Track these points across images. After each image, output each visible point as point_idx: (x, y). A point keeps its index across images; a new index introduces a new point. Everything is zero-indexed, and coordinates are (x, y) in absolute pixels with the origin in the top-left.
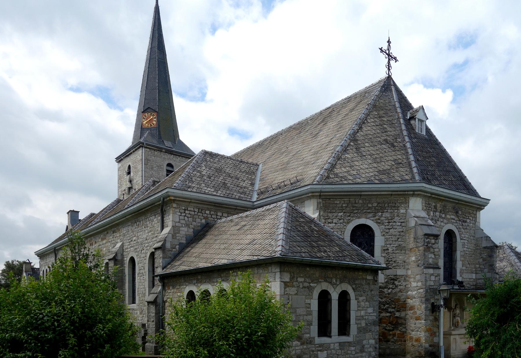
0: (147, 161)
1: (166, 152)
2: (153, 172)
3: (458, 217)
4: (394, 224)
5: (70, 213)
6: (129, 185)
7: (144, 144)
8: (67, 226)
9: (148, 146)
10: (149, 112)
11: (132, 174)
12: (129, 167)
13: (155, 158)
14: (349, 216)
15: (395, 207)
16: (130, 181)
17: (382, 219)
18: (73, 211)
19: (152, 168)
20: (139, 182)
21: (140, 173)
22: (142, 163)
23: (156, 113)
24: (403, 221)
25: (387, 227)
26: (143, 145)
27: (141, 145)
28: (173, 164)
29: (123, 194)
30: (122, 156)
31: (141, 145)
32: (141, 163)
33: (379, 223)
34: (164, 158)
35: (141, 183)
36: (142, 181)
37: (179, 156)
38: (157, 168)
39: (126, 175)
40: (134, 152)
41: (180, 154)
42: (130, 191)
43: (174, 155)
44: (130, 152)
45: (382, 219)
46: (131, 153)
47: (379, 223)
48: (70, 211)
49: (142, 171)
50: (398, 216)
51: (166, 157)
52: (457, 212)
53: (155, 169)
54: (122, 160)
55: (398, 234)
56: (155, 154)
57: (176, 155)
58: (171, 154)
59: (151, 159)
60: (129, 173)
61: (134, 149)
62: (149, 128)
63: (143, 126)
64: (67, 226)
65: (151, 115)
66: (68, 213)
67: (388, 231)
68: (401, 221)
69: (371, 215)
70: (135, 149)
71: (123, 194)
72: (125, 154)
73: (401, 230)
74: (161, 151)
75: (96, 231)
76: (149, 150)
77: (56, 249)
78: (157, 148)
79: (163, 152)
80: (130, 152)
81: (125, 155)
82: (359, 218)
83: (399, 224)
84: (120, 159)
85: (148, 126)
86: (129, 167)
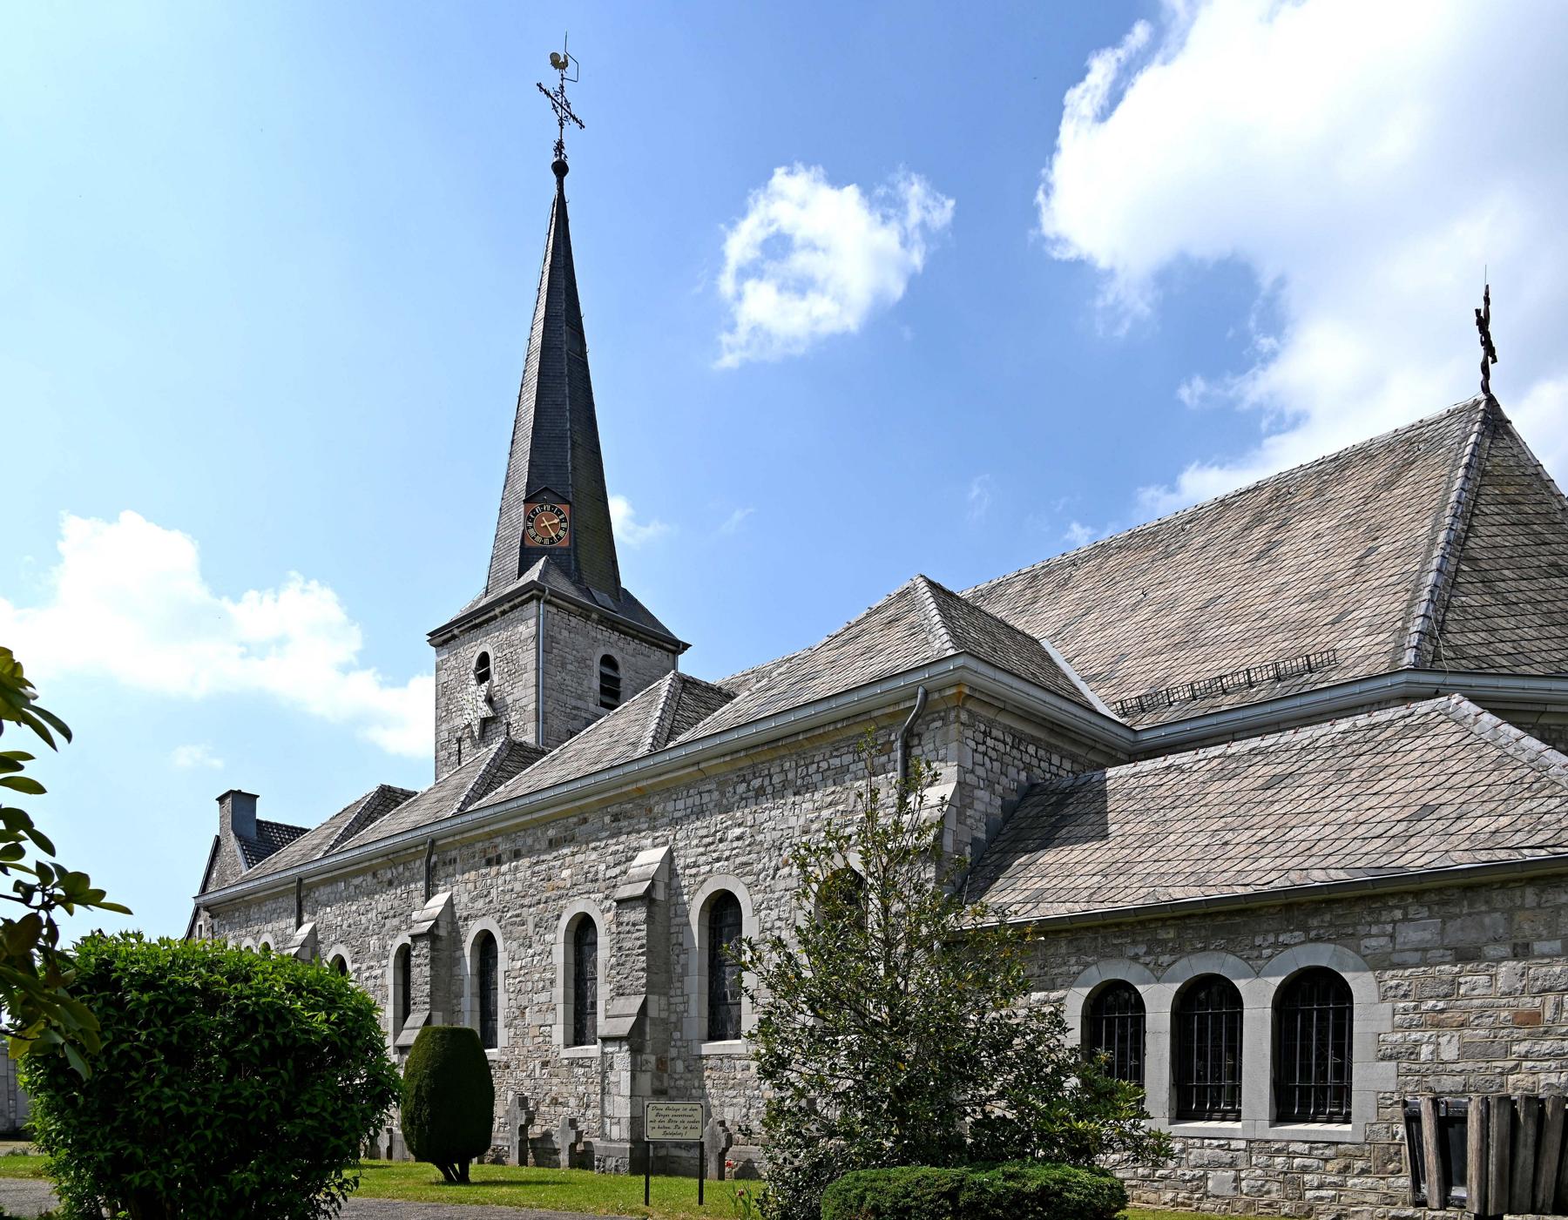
0: (546, 643)
1: (600, 622)
2: (567, 678)
5: (228, 801)
6: (486, 711)
9: (554, 599)
11: (495, 678)
12: (484, 659)
13: (572, 635)
16: (489, 700)
19: (563, 665)
20: (523, 703)
21: (530, 677)
22: (537, 648)
23: (568, 506)
26: (541, 594)
27: (534, 592)
29: (459, 740)
30: (458, 627)
31: (534, 592)
34: (595, 640)
35: (532, 706)
36: (537, 701)
38: (576, 664)
39: (474, 682)
40: (504, 613)
42: (488, 729)
43: (621, 632)
44: (492, 614)
46: (495, 617)
48: (231, 792)
49: (537, 669)
51: (599, 636)
53: (569, 667)
54: (454, 637)
56: (572, 624)
57: (626, 634)
58: (614, 629)
59: (560, 637)
61: (506, 606)
62: (545, 549)
63: (526, 542)
64: (218, 837)
65: (551, 511)
66: (221, 799)
70: (512, 603)
71: (459, 740)
72: (471, 621)
74: (588, 618)
75: (528, 817)
76: (554, 610)
77: (306, 881)
78: (579, 607)
79: (593, 621)
80: (492, 614)
81: (468, 623)
84: (449, 635)
85: (542, 543)
86: (484, 659)
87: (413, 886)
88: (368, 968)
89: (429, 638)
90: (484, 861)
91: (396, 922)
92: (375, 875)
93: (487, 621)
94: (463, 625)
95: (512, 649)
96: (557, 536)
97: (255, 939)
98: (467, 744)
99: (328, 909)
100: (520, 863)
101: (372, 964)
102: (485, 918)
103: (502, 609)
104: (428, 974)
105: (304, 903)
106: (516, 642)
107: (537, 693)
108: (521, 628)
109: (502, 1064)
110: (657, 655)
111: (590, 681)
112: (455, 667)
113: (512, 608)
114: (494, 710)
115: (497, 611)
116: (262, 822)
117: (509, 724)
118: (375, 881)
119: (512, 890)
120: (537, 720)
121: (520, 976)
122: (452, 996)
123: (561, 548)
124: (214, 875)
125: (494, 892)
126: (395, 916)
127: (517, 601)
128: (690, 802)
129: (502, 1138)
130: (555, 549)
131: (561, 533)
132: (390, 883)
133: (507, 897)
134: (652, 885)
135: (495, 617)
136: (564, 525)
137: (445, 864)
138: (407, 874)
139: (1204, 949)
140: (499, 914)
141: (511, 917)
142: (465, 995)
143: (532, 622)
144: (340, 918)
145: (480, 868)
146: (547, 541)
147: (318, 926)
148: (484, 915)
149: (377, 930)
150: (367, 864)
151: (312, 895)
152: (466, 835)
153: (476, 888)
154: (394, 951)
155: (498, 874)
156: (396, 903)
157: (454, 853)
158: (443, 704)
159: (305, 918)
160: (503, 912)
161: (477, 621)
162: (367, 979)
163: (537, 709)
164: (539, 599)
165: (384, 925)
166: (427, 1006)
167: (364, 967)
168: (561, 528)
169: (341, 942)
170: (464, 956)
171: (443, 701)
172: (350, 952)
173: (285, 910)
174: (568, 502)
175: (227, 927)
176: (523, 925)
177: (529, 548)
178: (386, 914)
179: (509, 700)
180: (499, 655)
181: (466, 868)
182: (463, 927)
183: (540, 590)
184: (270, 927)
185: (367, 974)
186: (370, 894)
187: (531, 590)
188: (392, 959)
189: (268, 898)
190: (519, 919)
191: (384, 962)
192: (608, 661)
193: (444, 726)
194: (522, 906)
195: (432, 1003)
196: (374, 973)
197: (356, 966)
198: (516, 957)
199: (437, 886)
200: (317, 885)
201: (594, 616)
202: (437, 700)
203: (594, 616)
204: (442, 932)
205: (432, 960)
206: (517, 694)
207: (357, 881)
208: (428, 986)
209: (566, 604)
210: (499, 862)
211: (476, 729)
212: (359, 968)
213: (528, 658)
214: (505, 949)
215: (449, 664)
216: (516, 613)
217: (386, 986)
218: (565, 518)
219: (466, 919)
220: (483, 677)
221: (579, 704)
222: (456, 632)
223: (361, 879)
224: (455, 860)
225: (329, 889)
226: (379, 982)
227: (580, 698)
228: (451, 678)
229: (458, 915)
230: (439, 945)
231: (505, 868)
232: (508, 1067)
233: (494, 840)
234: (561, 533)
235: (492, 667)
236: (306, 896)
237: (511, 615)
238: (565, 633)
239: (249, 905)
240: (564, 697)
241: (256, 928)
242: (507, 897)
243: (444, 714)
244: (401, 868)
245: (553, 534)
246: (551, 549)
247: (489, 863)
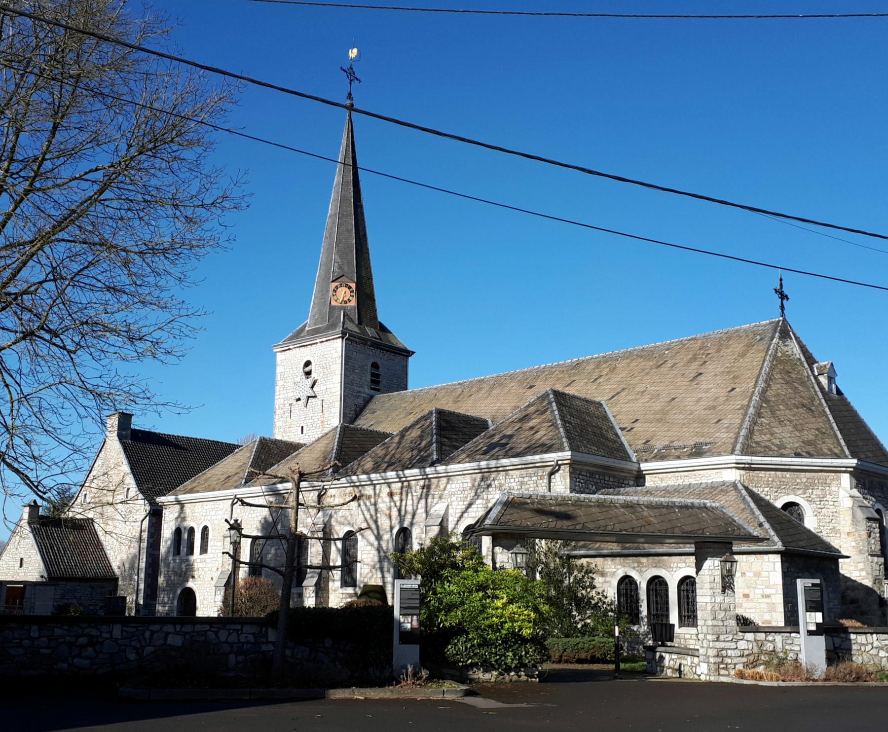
3: (883, 493)
4: (826, 503)
11: (314, 375)
14: (776, 492)
15: (826, 483)
17: (813, 496)
20: (333, 390)
24: (835, 500)
25: (818, 506)
28: (379, 363)
33: (810, 501)
34: (369, 355)
37: (387, 351)
43: (381, 349)
45: (813, 496)
46: (317, 343)
47: (810, 501)
50: (830, 494)
52: (882, 489)
54: (289, 349)
55: (831, 514)
58: (378, 348)
60: (308, 374)
67: (820, 510)
68: (834, 500)
69: (800, 492)
73: (835, 510)
74: (365, 344)
82: (788, 494)
83: (832, 503)
86: (308, 363)
93: (311, 344)
103: (321, 340)
110: (399, 358)
113: (327, 341)
127: (330, 338)
128: (458, 486)
134: (442, 520)
135: (317, 343)
139: (655, 567)
161: (305, 344)
192: (375, 365)
221: (361, 389)
222: (291, 347)
227: (361, 386)
238: (355, 353)
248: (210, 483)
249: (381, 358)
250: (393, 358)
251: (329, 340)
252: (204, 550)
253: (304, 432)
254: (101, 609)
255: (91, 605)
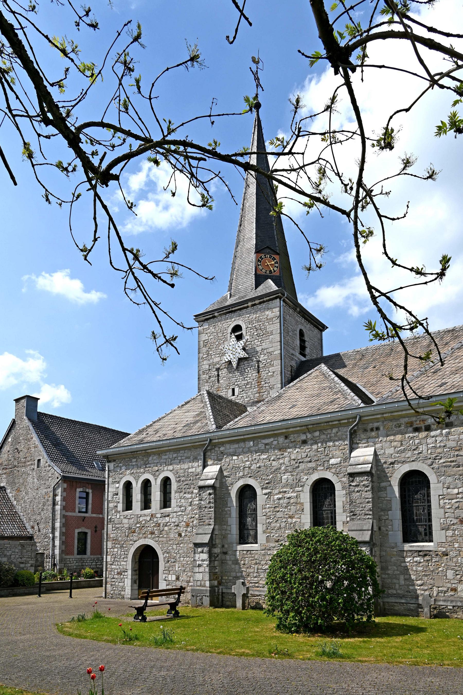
1: (299, 313)
2: (289, 339)
6: (243, 354)
7: (284, 296)
8: (14, 420)
9: (286, 299)
10: (268, 254)
11: (246, 337)
12: (237, 328)
18: (28, 397)
23: (278, 256)
27: (280, 294)
30: (218, 312)
31: (280, 294)
32: (278, 321)
36: (281, 350)
40: (253, 305)
41: (310, 319)
43: (305, 319)
44: (246, 305)
49: (281, 333)
53: (290, 334)
54: (214, 317)
58: (303, 317)
61: (257, 302)
62: (267, 276)
63: (257, 272)
66: (17, 401)
72: (230, 309)
74: (295, 310)
80: (246, 305)
84: (211, 316)
85: (266, 273)
86: (237, 328)
87: (331, 444)
88: (280, 492)
89: (195, 317)
90: (410, 429)
91: (312, 465)
92: (286, 437)
93: (240, 309)
94: (223, 311)
95: (261, 323)
96: (273, 270)
97: (154, 475)
98: (224, 372)
99: (235, 458)
100: (452, 430)
101: (285, 490)
102: (413, 463)
104: (371, 496)
105: (208, 453)
106: (264, 320)
107: (281, 345)
108: (267, 313)
109: (440, 553)
111: (296, 342)
112: (213, 332)
113: (260, 303)
114: (247, 354)
115: (250, 304)
116: (40, 413)
117: (258, 362)
118: (286, 441)
119: (444, 446)
120: (281, 359)
121: (457, 498)
122: (379, 510)
123: (276, 276)
124: (10, 440)
125: (423, 448)
126: (310, 462)
129: (444, 601)
130: (273, 276)
131: (275, 269)
132: (304, 442)
133: (439, 450)
135: (248, 307)
136: (277, 265)
137: (365, 430)
138: (323, 437)
140: (431, 460)
141: (444, 463)
142: (393, 508)
143: (278, 309)
144: (248, 463)
145: (406, 433)
146: (268, 272)
147: (223, 468)
148: (413, 461)
149: (290, 470)
150: (284, 431)
151: (216, 449)
152: (393, 414)
153: (402, 445)
154: (310, 482)
155: (427, 436)
156: (312, 453)
157: (376, 425)
158: (204, 351)
159: (210, 462)
160: (435, 459)
161: (233, 309)
162: (279, 499)
163: (281, 354)
164: (280, 299)
165: (298, 467)
166: (370, 517)
167: (277, 491)
168: (275, 266)
169: (250, 477)
170: (390, 485)
171: (204, 350)
172: (260, 483)
173: (188, 458)
174: (278, 254)
175: (124, 468)
176: (459, 467)
177: (259, 275)
178: (301, 460)
179: (259, 349)
180: (249, 326)
181: (389, 433)
182: (388, 468)
183: (282, 294)
184: (171, 467)
185: (280, 496)
186: (282, 449)
187: (278, 293)
188: (307, 489)
189: (170, 451)
190: (454, 463)
191: (300, 489)
193: (205, 362)
194: (457, 456)
195: (373, 514)
196: (288, 495)
197: (265, 491)
198: (451, 486)
199: (358, 444)
200: (223, 444)
201: (298, 309)
202: (199, 349)
203: (298, 309)
204: (374, 472)
205: (372, 488)
206: (264, 345)
207: (267, 441)
208: (371, 504)
209: (290, 302)
210: (428, 428)
211: (234, 364)
212: (270, 492)
213: (275, 327)
214: (439, 482)
215: (209, 331)
216: (264, 305)
217: (302, 504)
218: (277, 262)
219: (392, 463)
220: (239, 338)
221: (293, 352)
222: (216, 314)
223: (272, 439)
224: (378, 429)
225: (236, 446)
226: (292, 501)
228: (210, 338)
229: (383, 461)
230: (375, 478)
231: (433, 433)
232: (447, 555)
233: (422, 417)
234: (275, 269)
235: (244, 332)
236: (210, 450)
237: (259, 306)
239: (148, 455)
240: (288, 348)
241: (156, 468)
242: (439, 450)
243: (206, 356)
244: (317, 434)
245: (272, 269)
246: (271, 276)
247: (417, 430)
248: (164, 432)
249: (307, 328)
250: (313, 329)
251: (264, 302)
252: (166, 503)
253: (236, 393)
254: (31, 566)
255: (23, 563)
